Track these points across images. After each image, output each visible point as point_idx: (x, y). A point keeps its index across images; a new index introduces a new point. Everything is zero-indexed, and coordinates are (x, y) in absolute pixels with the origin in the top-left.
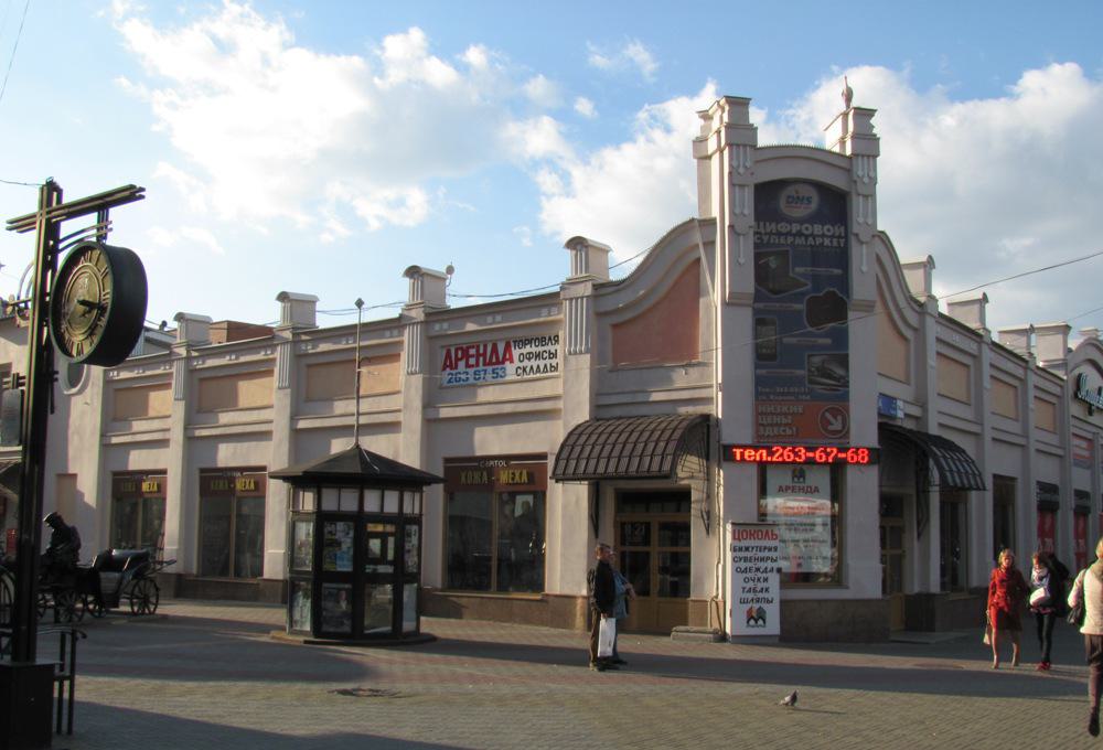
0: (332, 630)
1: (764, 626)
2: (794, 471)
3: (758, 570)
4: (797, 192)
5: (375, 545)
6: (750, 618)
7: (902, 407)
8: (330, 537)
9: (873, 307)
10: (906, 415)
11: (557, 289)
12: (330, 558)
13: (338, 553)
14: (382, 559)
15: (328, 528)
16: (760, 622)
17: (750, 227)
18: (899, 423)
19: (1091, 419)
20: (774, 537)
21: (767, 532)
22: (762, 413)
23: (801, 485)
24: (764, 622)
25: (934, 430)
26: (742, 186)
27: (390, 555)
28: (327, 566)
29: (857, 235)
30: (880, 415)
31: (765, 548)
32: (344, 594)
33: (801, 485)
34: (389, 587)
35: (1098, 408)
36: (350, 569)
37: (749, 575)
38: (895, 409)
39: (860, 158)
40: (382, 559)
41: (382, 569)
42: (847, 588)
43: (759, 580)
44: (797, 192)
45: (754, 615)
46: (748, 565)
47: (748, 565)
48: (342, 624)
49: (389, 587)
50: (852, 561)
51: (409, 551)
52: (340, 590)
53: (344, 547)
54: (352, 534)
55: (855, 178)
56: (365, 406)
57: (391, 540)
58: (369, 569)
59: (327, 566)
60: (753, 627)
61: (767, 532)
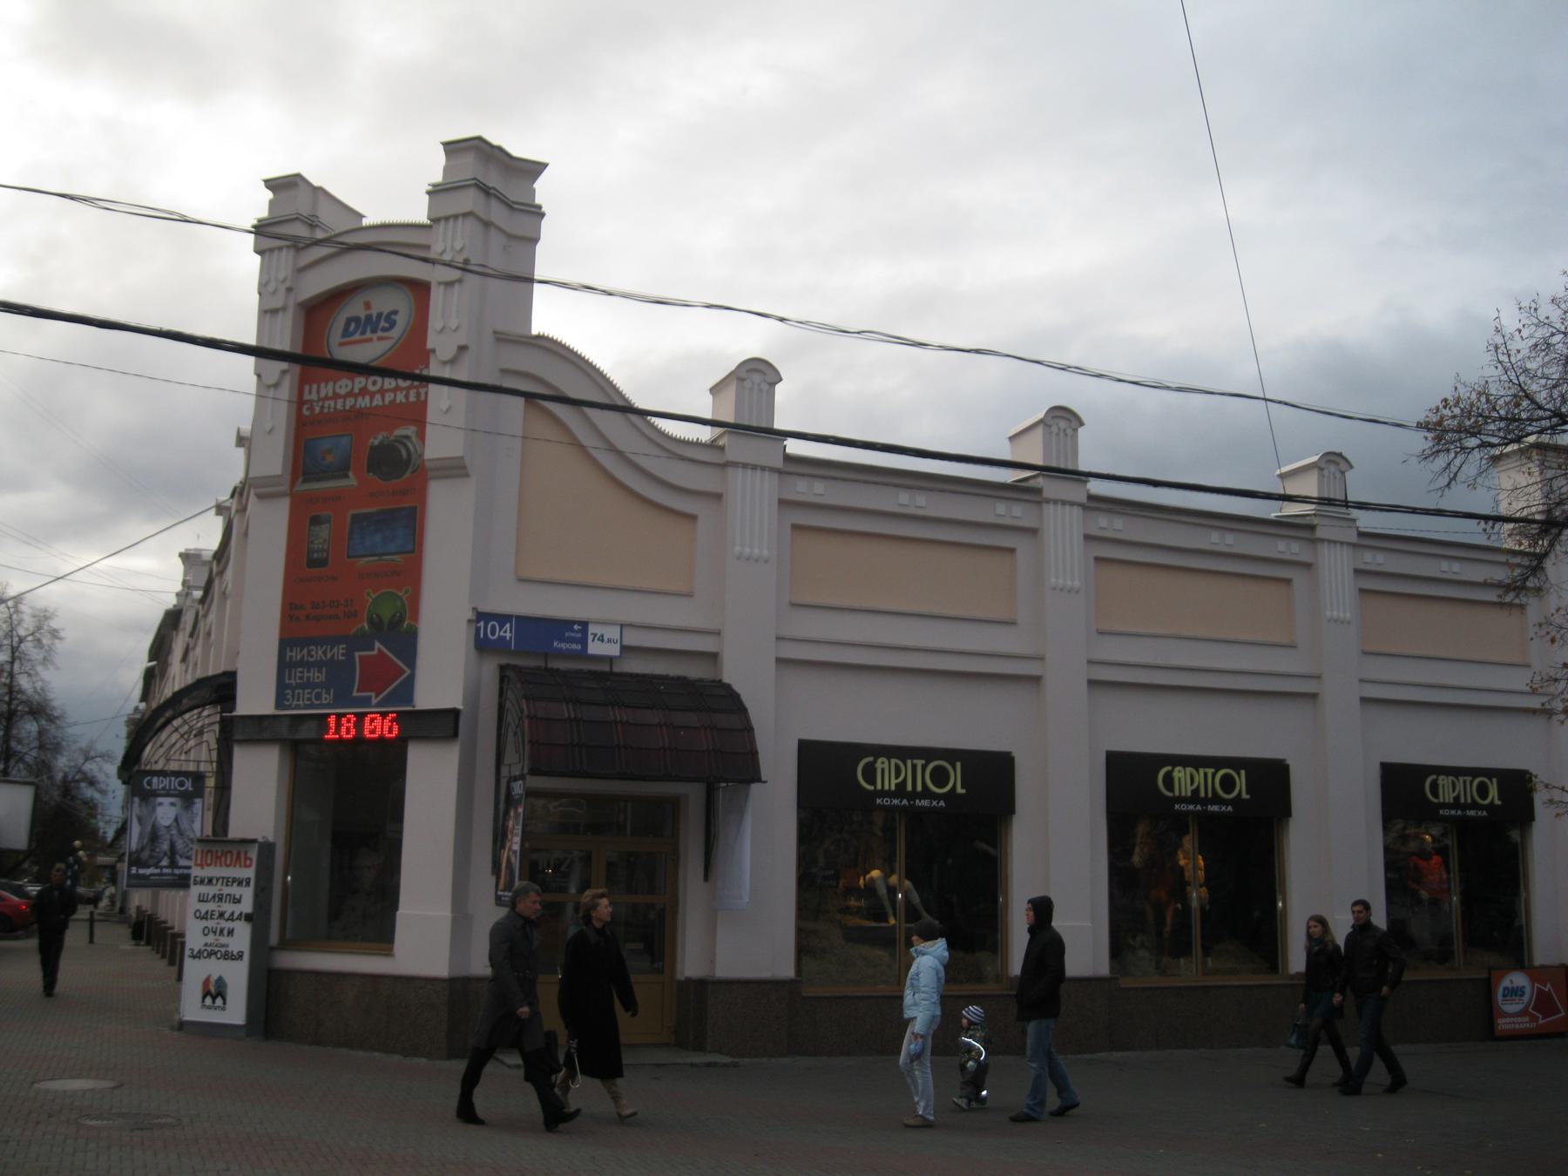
1: (224, 1009)
3: (221, 915)
6: (206, 993)
16: (219, 1001)
21: (239, 853)
24: (225, 1003)
31: (234, 880)
37: (211, 924)
43: (222, 931)
45: (213, 989)
46: (211, 906)
47: (211, 906)
60: (209, 1008)
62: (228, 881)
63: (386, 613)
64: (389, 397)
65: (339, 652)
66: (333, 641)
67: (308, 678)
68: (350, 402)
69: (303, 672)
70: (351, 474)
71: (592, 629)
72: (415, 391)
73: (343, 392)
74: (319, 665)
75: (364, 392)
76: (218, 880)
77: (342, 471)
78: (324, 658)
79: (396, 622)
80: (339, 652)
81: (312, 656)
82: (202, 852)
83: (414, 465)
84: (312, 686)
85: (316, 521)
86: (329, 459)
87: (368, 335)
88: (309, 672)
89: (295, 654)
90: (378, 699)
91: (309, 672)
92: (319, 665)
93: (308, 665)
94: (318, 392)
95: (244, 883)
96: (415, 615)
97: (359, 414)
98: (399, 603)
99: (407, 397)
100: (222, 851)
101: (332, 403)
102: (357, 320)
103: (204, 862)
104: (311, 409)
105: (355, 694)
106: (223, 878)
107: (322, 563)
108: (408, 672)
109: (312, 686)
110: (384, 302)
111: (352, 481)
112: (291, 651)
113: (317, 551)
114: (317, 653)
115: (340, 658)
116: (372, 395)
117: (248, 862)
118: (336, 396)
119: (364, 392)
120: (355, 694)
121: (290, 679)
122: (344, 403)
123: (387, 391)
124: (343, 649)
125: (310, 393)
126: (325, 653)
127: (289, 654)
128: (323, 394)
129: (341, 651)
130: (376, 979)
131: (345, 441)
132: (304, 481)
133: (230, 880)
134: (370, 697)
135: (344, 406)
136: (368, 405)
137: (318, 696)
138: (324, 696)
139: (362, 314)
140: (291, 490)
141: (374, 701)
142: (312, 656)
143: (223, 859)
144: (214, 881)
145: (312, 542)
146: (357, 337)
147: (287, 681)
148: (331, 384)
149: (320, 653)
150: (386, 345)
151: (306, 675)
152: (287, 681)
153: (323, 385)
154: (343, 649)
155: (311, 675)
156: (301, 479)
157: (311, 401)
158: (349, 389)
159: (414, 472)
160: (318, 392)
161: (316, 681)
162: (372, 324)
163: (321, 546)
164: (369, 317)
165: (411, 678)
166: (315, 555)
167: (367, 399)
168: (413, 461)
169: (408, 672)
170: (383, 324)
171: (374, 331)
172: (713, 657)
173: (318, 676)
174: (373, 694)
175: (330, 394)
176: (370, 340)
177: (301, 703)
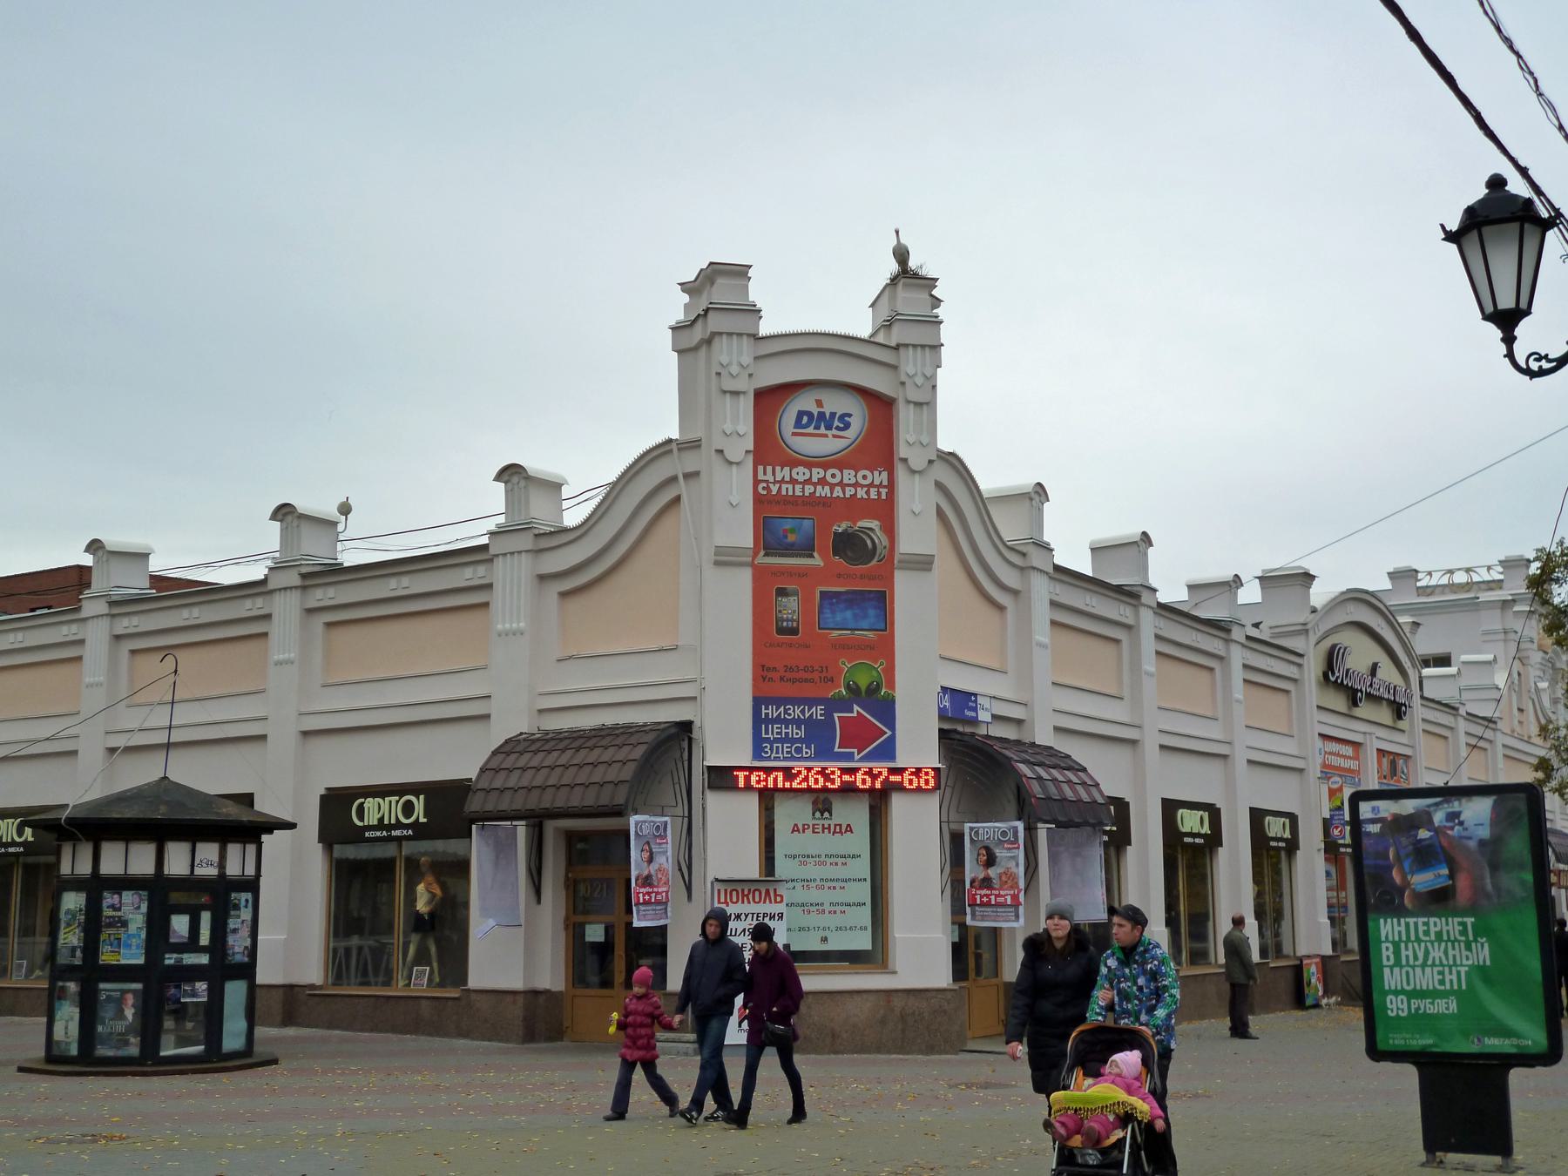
0: (110, 1053)
2: (815, 803)
4: (819, 403)
5: (180, 924)
7: (987, 705)
8: (111, 913)
9: (932, 563)
10: (994, 717)
11: (485, 540)
12: (111, 945)
13: (123, 937)
14: (192, 944)
15: (109, 899)
17: (747, 452)
18: (982, 731)
19: (1358, 712)
20: (778, 898)
21: (768, 892)
22: (769, 721)
23: (826, 823)
25: (1043, 736)
26: (736, 393)
27: (205, 939)
28: (107, 957)
29: (905, 460)
30: (943, 716)
32: (130, 999)
33: (826, 823)
34: (202, 986)
35: (1369, 696)
36: (141, 961)
38: (975, 709)
39: (911, 349)
40: (192, 944)
41: (190, 959)
42: (895, 973)
44: (819, 403)
48: (127, 1043)
49: (202, 986)
50: (900, 931)
51: (235, 931)
52: (124, 992)
53: (132, 928)
54: (144, 907)
55: (903, 378)
56: (183, 715)
57: (206, 917)
58: (170, 959)
59: (107, 957)
61: (768, 892)
62: (758, 917)
63: (863, 681)
64: (849, 492)
65: (818, 712)
66: (811, 702)
67: (787, 733)
68: (809, 489)
69: (781, 728)
70: (815, 554)
71: (980, 700)
72: (876, 489)
73: (801, 478)
74: (798, 722)
75: (822, 482)
76: (746, 916)
77: (807, 549)
78: (803, 718)
79: (873, 690)
80: (818, 712)
81: (790, 715)
82: (726, 890)
83: (880, 556)
84: (793, 741)
85: (782, 592)
86: (791, 538)
87: (823, 430)
88: (787, 728)
89: (771, 711)
90: (861, 755)
91: (787, 728)
92: (798, 722)
93: (786, 722)
94: (774, 473)
95: (777, 918)
96: (891, 684)
97: (825, 502)
98: (875, 674)
99: (868, 493)
100: (749, 890)
101: (790, 487)
102: (810, 415)
103: (728, 900)
104: (767, 488)
105: (836, 750)
106: (753, 914)
107: (794, 631)
108: (889, 733)
109: (793, 741)
110: (836, 403)
111: (817, 561)
112: (767, 708)
113: (787, 620)
114: (794, 711)
115: (819, 718)
116: (832, 487)
117: (779, 899)
118: (793, 482)
119: (822, 482)
120: (836, 750)
121: (767, 733)
122: (803, 488)
123: (849, 485)
124: (821, 709)
125: (765, 474)
126: (803, 712)
127: (764, 711)
128: (779, 478)
129: (819, 712)
130: (889, 993)
131: (807, 523)
132: (766, 555)
133: (762, 915)
134: (853, 753)
135: (803, 491)
136: (829, 495)
137: (799, 750)
138: (804, 750)
139: (815, 411)
140: (753, 560)
141: (857, 757)
142: (790, 715)
143: (751, 896)
144: (743, 917)
145: (780, 612)
146: (810, 430)
147: (764, 736)
148: (787, 469)
149: (797, 712)
150: (841, 443)
151: (784, 731)
152: (764, 736)
153: (778, 469)
154: (821, 709)
155: (790, 731)
156: (762, 553)
157: (767, 482)
158: (807, 477)
159: (881, 560)
160: (774, 473)
161: (795, 736)
162: (824, 421)
163: (790, 616)
164: (822, 415)
165: (892, 739)
166: (785, 624)
167: (827, 489)
168: (878, 551)
169: (889, 733)
170: (836, 423)
171: (829, 427)
172: (1019, 722)
173: (798, 733)
174: (856, 751)
175: (787, 478)
176: (826, 436)
177: (780, 755)
